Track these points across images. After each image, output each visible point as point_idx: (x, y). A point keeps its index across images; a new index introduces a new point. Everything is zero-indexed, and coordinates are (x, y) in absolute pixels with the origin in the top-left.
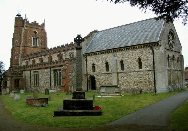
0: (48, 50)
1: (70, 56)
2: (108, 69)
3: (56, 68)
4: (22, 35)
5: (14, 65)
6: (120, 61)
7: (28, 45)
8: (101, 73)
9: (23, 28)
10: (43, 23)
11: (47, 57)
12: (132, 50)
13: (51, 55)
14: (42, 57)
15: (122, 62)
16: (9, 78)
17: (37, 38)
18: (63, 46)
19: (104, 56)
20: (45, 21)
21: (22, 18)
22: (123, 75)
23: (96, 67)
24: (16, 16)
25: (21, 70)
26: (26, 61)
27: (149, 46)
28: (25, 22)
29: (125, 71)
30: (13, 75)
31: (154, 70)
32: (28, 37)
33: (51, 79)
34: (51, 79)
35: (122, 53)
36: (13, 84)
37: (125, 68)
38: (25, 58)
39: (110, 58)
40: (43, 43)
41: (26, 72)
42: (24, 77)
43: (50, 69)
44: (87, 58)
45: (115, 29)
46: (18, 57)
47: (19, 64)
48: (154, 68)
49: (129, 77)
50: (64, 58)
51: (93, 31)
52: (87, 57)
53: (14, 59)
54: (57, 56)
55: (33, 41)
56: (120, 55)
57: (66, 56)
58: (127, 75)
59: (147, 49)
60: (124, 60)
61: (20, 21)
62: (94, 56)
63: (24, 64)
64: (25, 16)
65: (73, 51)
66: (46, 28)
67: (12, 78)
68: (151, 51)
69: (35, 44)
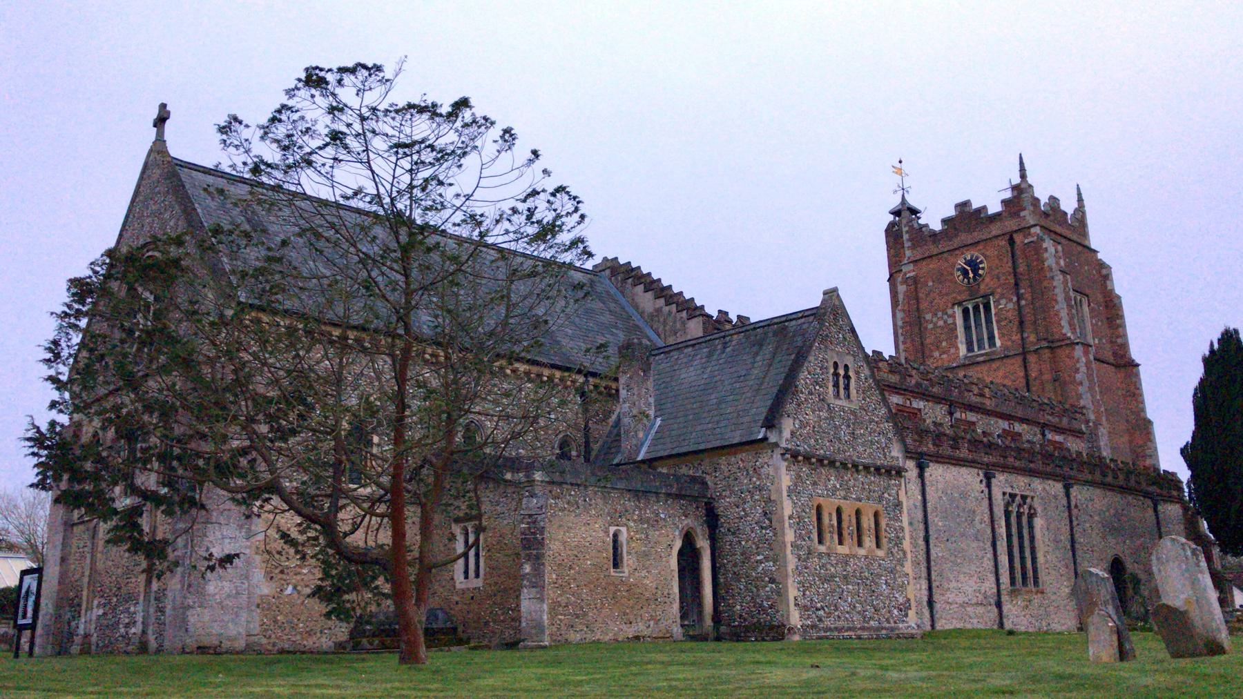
10: (1015, 188)
32: (928, 317)
55: (967, 328)
69: (980, 341)
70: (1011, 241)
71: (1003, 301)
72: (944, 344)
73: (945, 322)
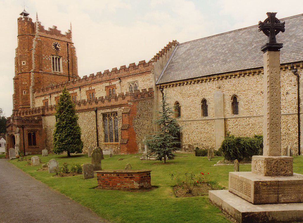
0: (80, 80)
1: (130, 88)
2: (205, 112)
3: (109, 111)
4: (33, 52)
5: (21, 107)
6: (231, 97)
7: (45, 69)
8: (191, 119)
9: (35, 39)
11: (84, 90)
12: (256, 76)
13: (93, 88)
14: (75, 91)
15: (235, 99)
16: (18, 129)
17: (60, 57)
18: (115, 70)
19: (198, 87)
20: (72, 28)
21: (31, 19)
22: (237, 123)
23: (182, 108)
24: (20, 16)
25: (37, 114)
26: (43, 98)
27: (292, 68)
28: (37, 26)
29: (241, 114)
30: (24, 125)
31: (299, 114)
32: (43, 55)
33: (97, 131)
34: (97, 131)
35: (234, 81)
36: (25, 141)
37: (241, 109)
38: (41, 93)
39: (210, 91)
40: (70, 68)
41: (47, 118)
42: (44, 128)
43: (96, 111)
44: (164, 92)
45: (213, 38)
46: (28, 92)
47: (31, 104)
48: (299, 108)
49: (247, 127)
50: (118, 92)
51: (171, 42)
52: (165, 89)
53: (20, 95)
54: (104, 89)
55: (53, 63)
56: (230, 86)
57: (122, 88)
58: (243, 122)
59: (287, 74)
60: (238, 95)
61: (27, 27)
62: (178, 87)
63: (39, 103)
64: (37, 15)
65: (137, 80)
66: (75, 40)
67: (23, 128)
68: (294, 78)
70: (68, 45)
71: (64, 60)
72: (48, 65)
73: (48, 59)
